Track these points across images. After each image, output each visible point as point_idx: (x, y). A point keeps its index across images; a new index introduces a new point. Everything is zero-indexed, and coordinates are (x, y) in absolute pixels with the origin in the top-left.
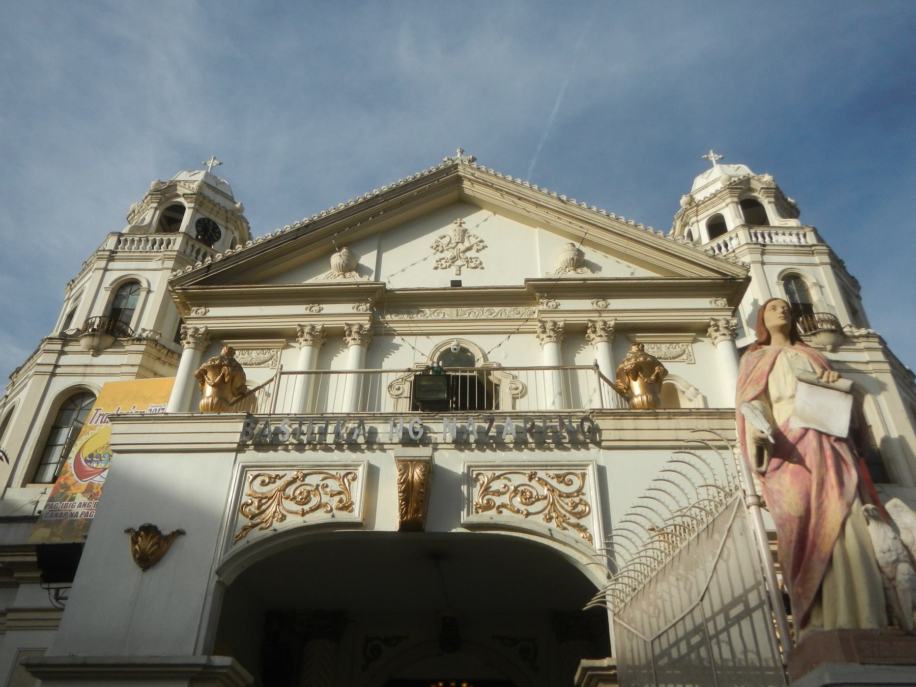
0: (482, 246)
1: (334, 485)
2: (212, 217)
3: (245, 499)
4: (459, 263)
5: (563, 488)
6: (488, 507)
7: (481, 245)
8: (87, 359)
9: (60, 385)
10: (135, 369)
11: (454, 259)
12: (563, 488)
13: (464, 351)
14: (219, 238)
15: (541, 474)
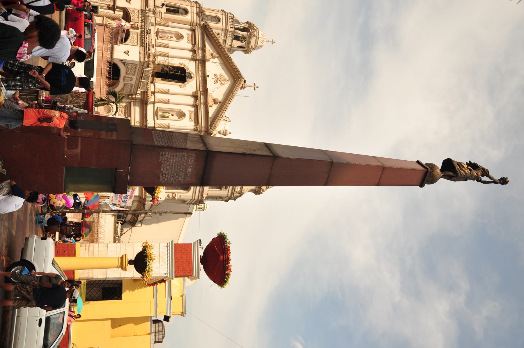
0: (221, 84)
1: (136, 19)
2: (247, 40)
3: (134, 10)
4: (216, 79)
5: (134, 42)
6: (132, 34)
7: (222, 84)
8: (195, 12)
9: (189, 8)
10: (192, 21)
11: (217, 78)
12: (134, 42)
13: (192, 77)
14: (241, 42)
15: (137, 40)
